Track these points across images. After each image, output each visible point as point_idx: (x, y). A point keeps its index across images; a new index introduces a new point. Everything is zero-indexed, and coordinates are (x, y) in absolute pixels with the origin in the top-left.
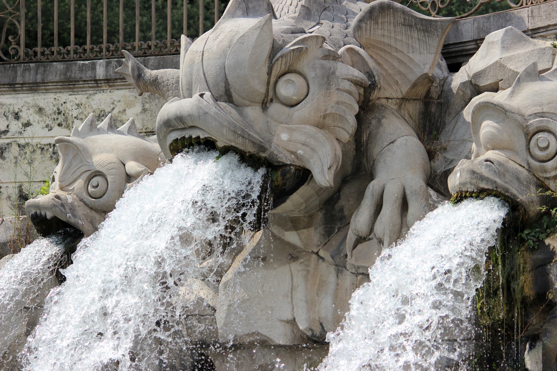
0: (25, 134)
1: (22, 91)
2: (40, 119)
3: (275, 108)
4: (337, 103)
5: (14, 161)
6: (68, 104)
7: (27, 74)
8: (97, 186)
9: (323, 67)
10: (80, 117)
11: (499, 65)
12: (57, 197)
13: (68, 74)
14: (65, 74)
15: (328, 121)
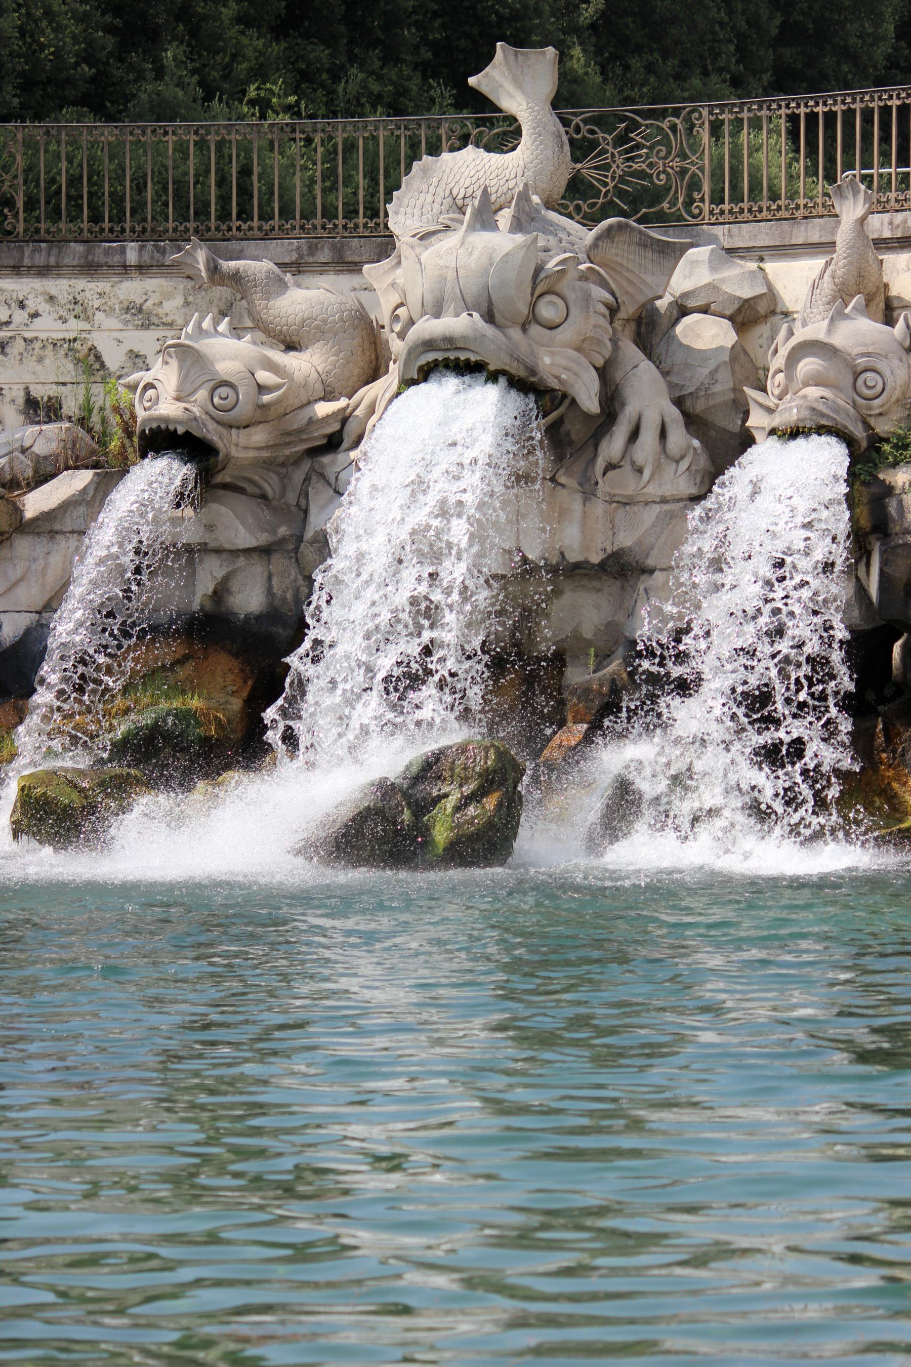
0: (32, 327)
1: (28, 275)
3: (535, 329)
4: (595, 326)
5: (18, 358)
6: (87, 292)
8: (226, 399)
10: (103, 308)
11: (712, 287)
12: (187, 409)
13: (90, 258)
14: (86, 258)
15: (586, 345)
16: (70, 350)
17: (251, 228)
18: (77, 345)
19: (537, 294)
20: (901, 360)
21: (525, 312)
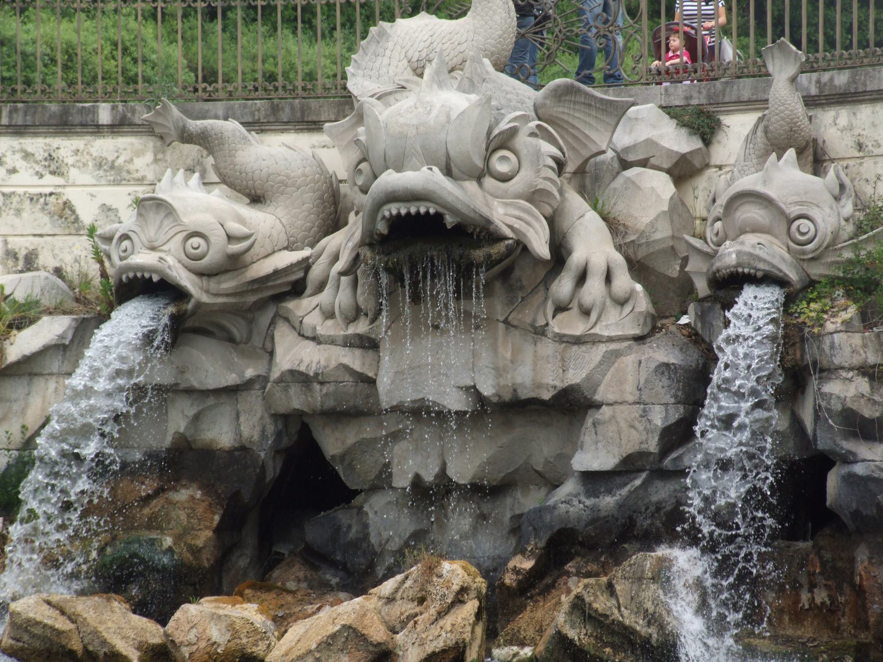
2: (28, 166)
3: (488, 181)
12: (161, 258)
17: (217, 90)
18: (52, 199)
19: (490, 150)
20: (832, 208)
21: (480, 163)
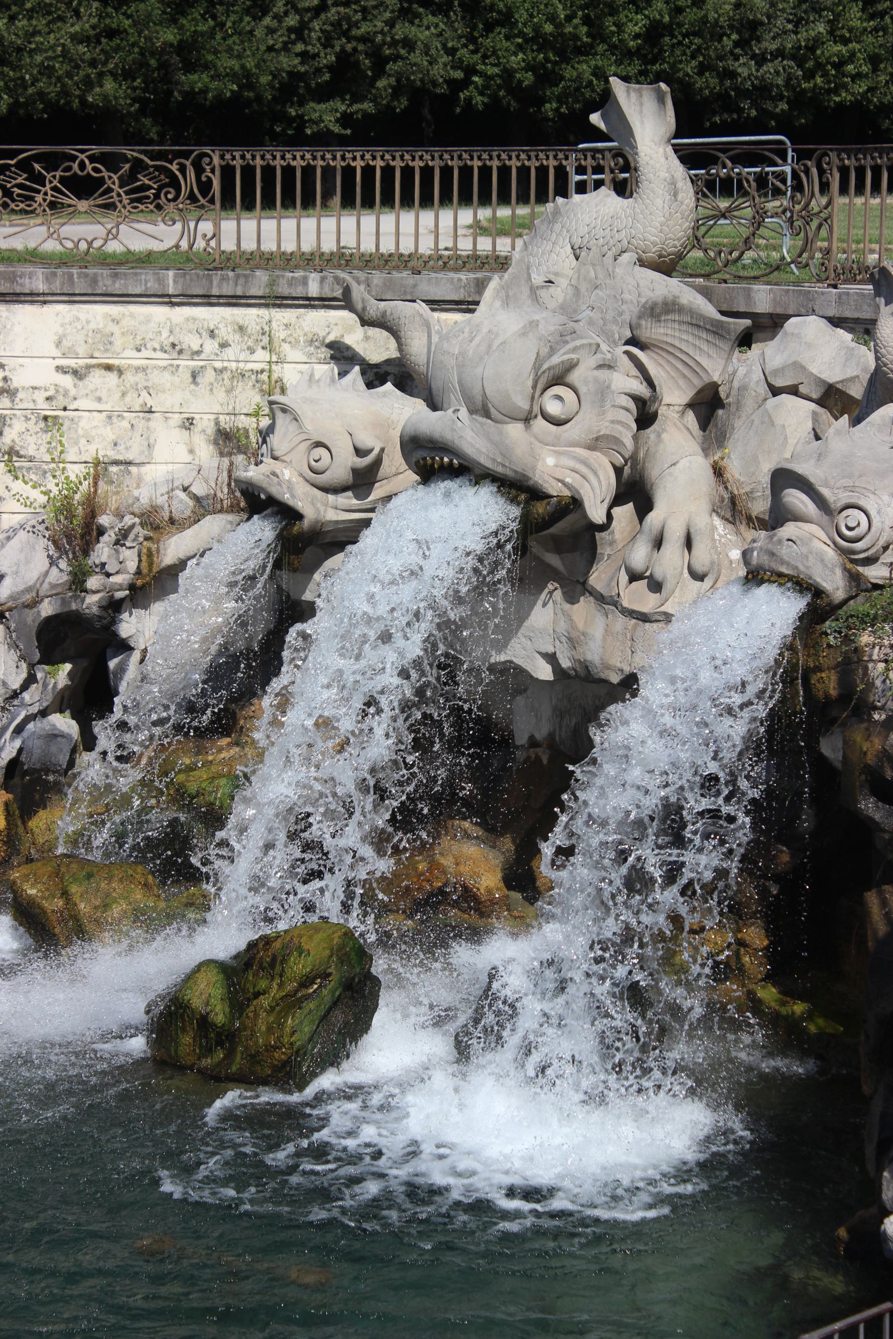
4: (612, 422)
7: (225, 285)
9: (596, 380)
10: (288, 340)
16: (257, 381)
21: (526, 406)
